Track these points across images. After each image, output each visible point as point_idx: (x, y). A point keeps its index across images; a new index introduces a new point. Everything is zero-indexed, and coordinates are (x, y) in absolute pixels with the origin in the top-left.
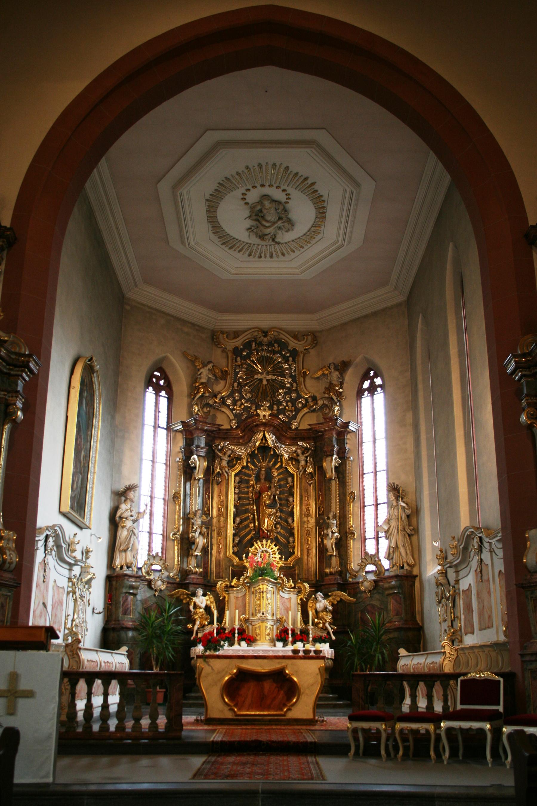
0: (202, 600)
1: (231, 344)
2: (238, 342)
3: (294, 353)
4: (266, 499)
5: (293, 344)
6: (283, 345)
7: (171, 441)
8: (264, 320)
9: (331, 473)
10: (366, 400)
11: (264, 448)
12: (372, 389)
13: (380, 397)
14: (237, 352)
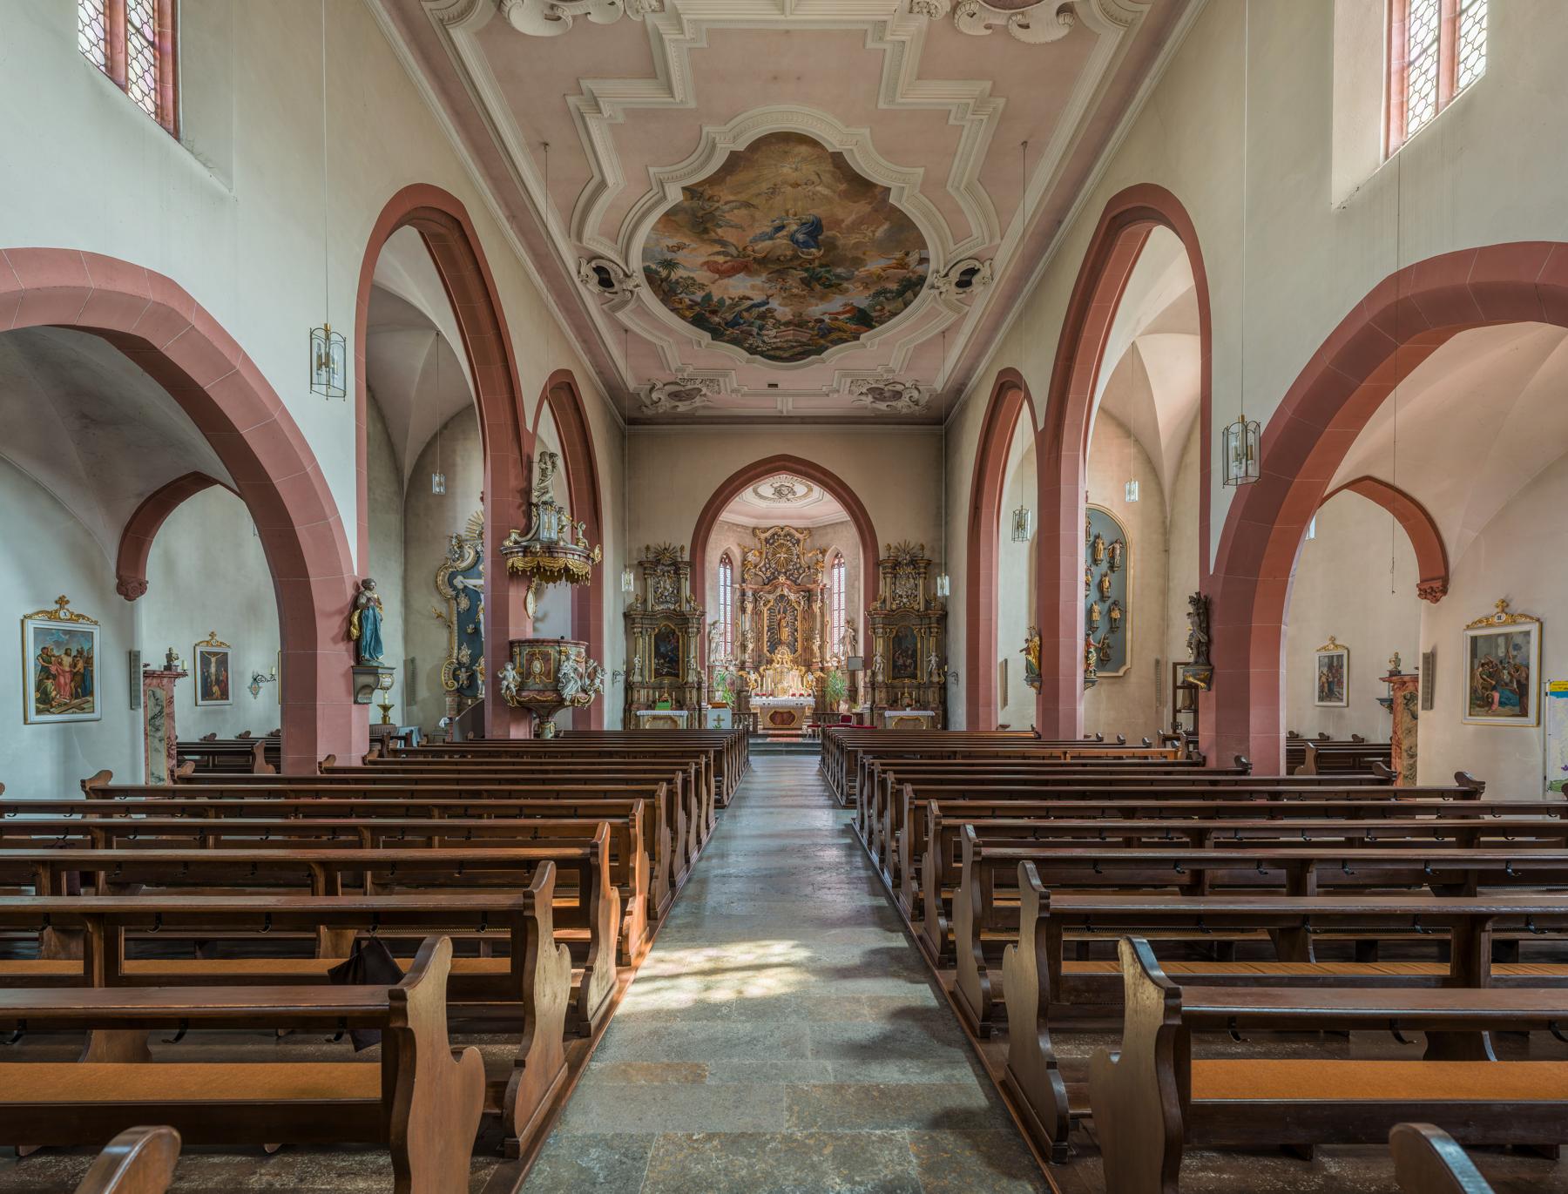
0: (753, 676)
1: (763, 536)
2: (768, 534)
3: (798, 541)
4: (783, 623)
5: (797, 535)
6: (792, 536)
7: (733, 593)
8: (782, 523)
9: (818, 611)
10: (836, 571)
11: (782, 596)
12: (839, 565)
13: (843, 570)
14: (767, 541)
